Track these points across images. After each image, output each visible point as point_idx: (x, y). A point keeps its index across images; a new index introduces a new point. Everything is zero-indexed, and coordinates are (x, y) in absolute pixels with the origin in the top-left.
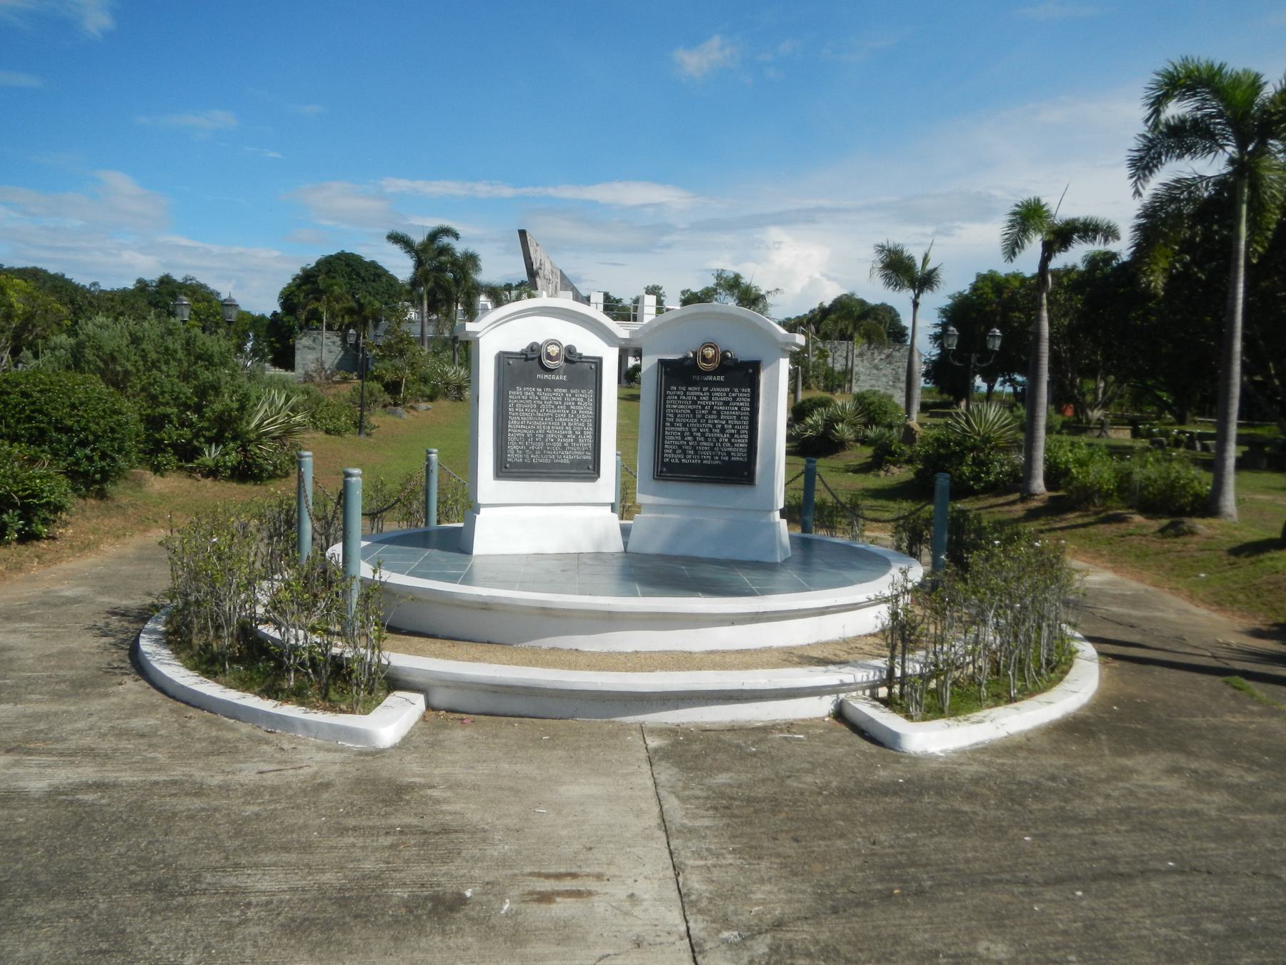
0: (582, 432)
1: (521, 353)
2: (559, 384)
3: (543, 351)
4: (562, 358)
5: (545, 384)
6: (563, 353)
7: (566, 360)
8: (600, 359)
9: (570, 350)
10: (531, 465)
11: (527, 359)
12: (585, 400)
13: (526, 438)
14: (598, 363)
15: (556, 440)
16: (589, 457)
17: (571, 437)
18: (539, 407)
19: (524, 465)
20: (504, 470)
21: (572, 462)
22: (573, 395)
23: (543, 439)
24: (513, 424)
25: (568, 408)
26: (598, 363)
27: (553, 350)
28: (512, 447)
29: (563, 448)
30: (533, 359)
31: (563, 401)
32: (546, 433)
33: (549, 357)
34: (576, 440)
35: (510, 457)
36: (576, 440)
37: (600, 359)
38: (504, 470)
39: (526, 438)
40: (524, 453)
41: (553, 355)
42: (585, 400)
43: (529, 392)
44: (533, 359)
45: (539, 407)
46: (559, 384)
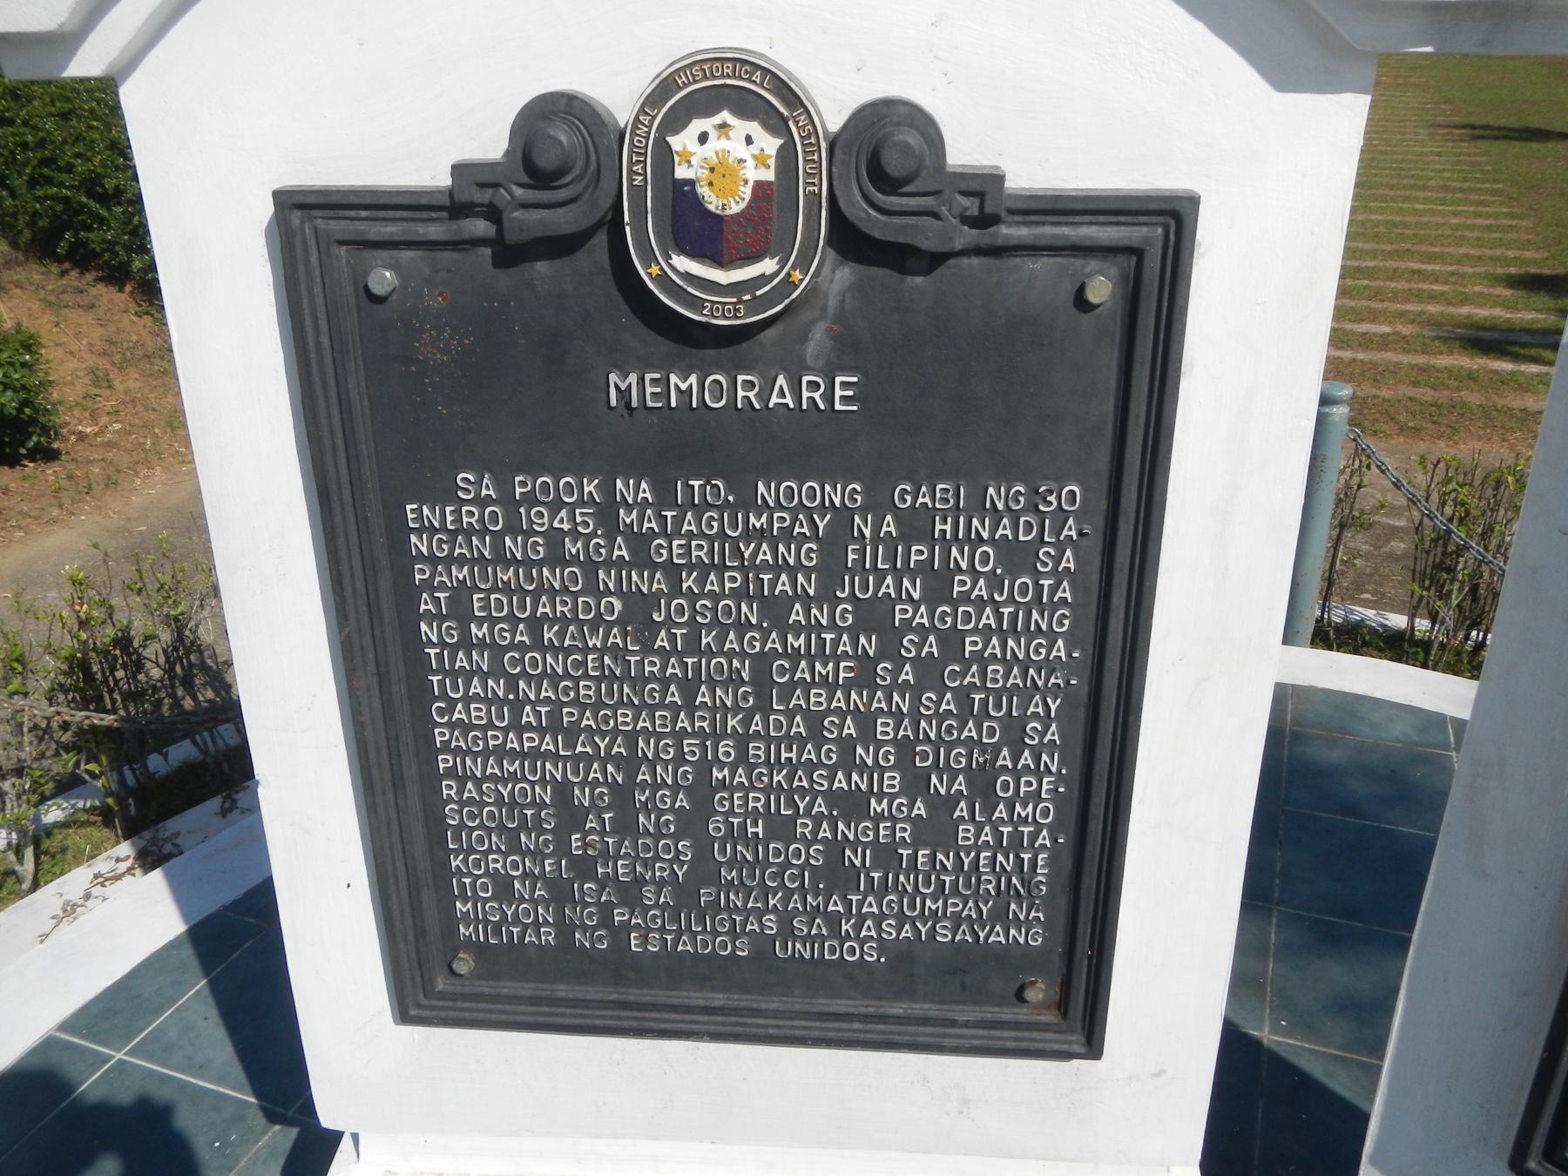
0: (983, 785)
1: (453, 206)
2: (800, 445)
3: (635, 172)
4: (809, 223)
5: (679, 448)
6: (813, 183)
7: (849, 240)
8: (1173, 219)
9: (887, 145)
10: (619, 966)
11: (509, 254)
12: (1016, 557)
13: (571, 816)
14: (1151, 244)
15: (782, 829)
16: (1029, 932)
17: (895, 812)
18: (639, 613)
19: (564, 960)
20: (437, 974)
21: (902, 957)
22: (916, 526)
23: (693, 823)
24: (463, 716)
25: (874, 616)
26: (1151, 244)
27: (728, 158)
28: (478, 863)
29: (836, 874)
30: (561, 246)
31: (831, 571)
32: (703, 791)
33: (693, 226)
34: (937, 830)
35: (475, 914)
36: (937, 830)
37: (1173, 219)
38: (437, 974)
39: (571, 816)
40: (560, 894)
41: (730, 202)
42: (1016, 557)
43: (564, 502)
44: (561, 246)
45: (639, 613)
46: (800, 445)
